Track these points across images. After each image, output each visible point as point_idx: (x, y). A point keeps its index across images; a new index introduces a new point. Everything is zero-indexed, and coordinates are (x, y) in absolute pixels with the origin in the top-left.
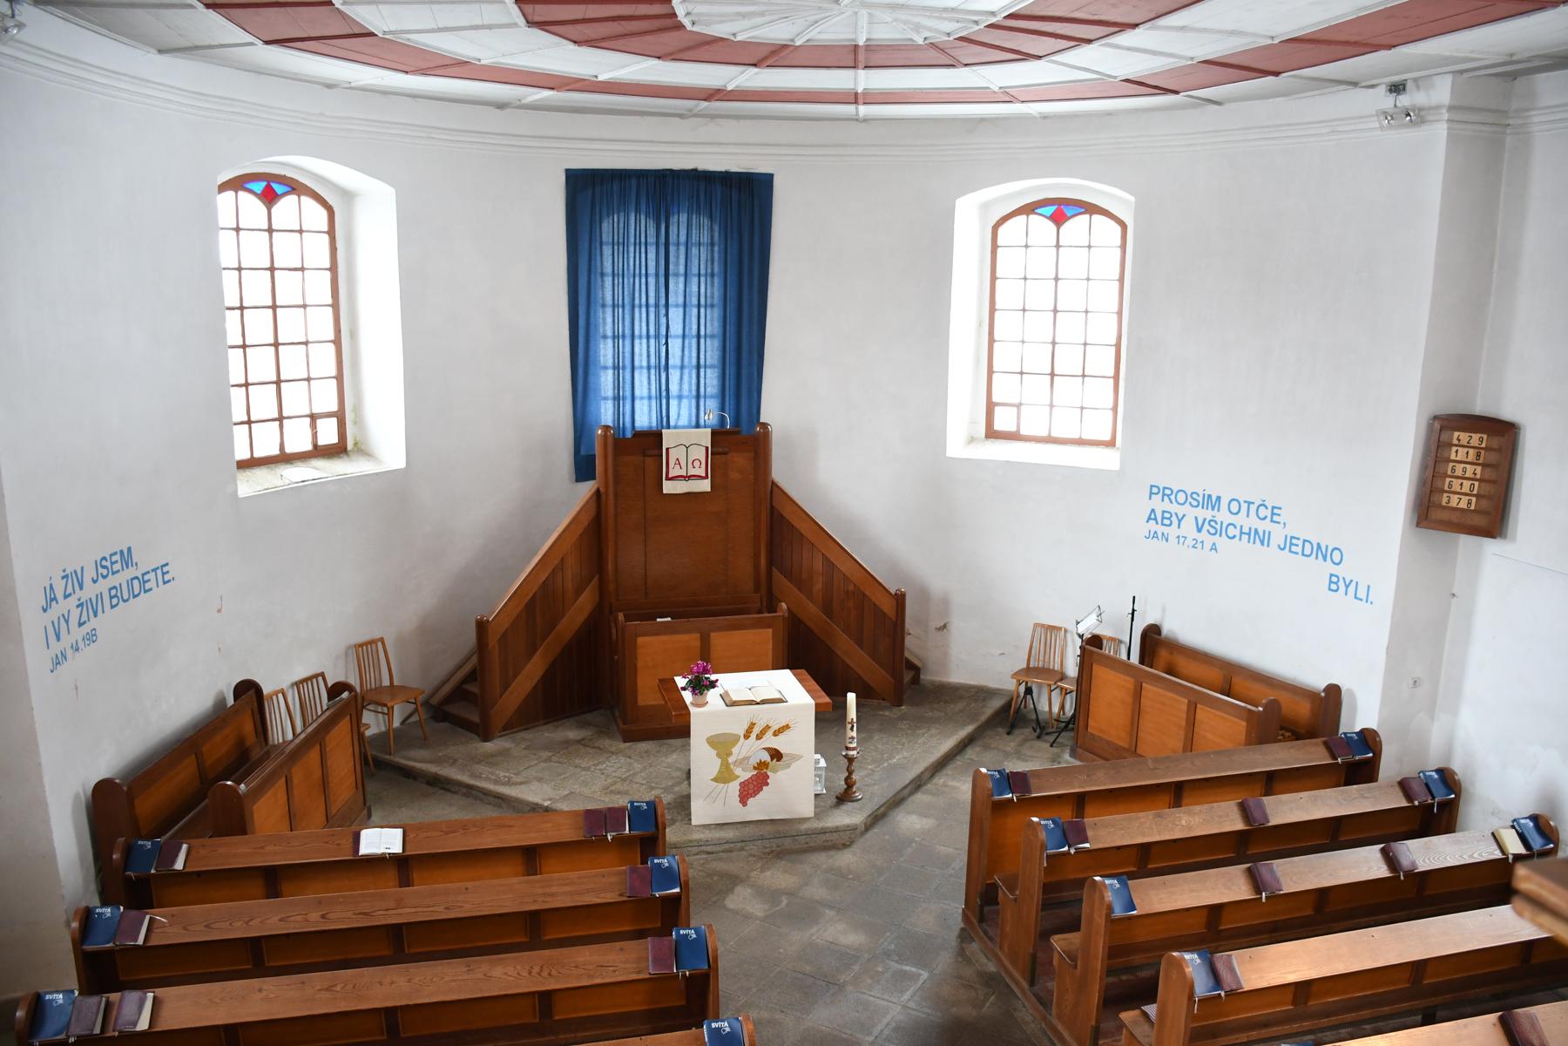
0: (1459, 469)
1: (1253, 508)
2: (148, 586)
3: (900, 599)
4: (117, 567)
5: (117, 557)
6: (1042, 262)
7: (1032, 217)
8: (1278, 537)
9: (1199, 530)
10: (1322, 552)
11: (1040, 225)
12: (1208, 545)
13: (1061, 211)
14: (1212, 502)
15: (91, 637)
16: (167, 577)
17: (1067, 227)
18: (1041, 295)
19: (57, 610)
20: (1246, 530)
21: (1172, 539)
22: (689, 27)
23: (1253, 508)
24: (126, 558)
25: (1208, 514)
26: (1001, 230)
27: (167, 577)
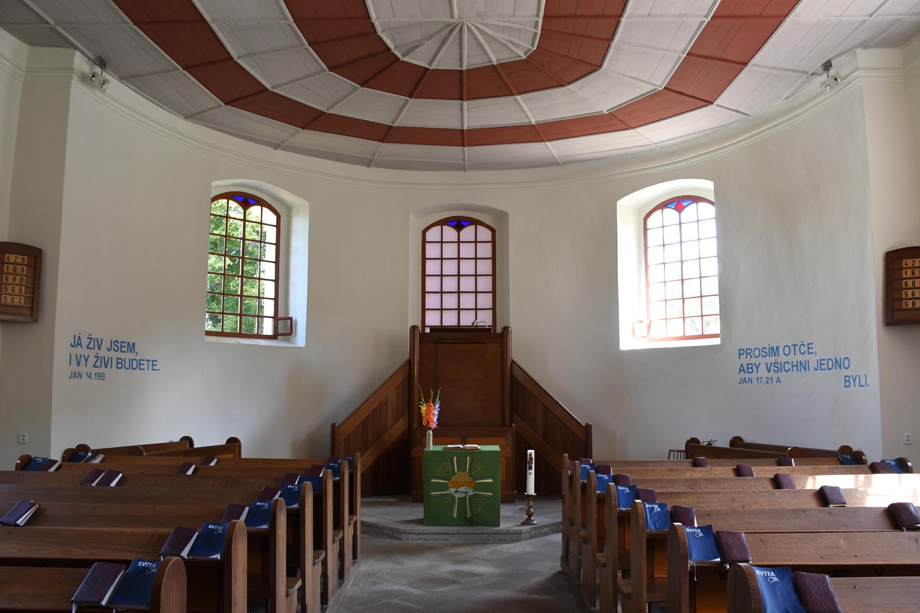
0: (910, 282)
1: (797, 348)
2: (142, 367)
3: (588, 428)
4: (123, 349)
5: (126, 345)
6: (672, 234)
7: (666, 211)
8: (813, 364)
9: (769, 371)
10: (838, 364)
11: (670, 214)
12: (775, 380)
13: (678, 203)
14: (774, 351)
15: (101, 376)
16: (155, 367)
17: (684, 213)
18: (673, 253)
19: (78, 351)
20: (795, 364)
21: (754, 380)
22: (402, 59)
23: (797, 348)
24: (131, 347)
25: (772, 359)
26: (649, 221)
27: (155, 367)
